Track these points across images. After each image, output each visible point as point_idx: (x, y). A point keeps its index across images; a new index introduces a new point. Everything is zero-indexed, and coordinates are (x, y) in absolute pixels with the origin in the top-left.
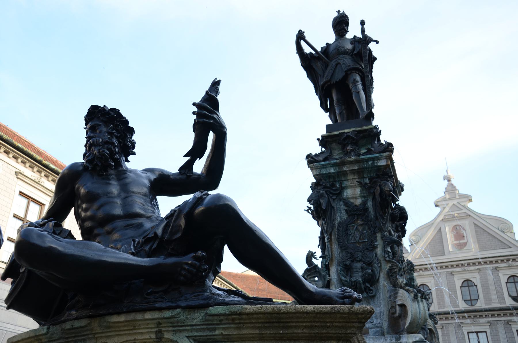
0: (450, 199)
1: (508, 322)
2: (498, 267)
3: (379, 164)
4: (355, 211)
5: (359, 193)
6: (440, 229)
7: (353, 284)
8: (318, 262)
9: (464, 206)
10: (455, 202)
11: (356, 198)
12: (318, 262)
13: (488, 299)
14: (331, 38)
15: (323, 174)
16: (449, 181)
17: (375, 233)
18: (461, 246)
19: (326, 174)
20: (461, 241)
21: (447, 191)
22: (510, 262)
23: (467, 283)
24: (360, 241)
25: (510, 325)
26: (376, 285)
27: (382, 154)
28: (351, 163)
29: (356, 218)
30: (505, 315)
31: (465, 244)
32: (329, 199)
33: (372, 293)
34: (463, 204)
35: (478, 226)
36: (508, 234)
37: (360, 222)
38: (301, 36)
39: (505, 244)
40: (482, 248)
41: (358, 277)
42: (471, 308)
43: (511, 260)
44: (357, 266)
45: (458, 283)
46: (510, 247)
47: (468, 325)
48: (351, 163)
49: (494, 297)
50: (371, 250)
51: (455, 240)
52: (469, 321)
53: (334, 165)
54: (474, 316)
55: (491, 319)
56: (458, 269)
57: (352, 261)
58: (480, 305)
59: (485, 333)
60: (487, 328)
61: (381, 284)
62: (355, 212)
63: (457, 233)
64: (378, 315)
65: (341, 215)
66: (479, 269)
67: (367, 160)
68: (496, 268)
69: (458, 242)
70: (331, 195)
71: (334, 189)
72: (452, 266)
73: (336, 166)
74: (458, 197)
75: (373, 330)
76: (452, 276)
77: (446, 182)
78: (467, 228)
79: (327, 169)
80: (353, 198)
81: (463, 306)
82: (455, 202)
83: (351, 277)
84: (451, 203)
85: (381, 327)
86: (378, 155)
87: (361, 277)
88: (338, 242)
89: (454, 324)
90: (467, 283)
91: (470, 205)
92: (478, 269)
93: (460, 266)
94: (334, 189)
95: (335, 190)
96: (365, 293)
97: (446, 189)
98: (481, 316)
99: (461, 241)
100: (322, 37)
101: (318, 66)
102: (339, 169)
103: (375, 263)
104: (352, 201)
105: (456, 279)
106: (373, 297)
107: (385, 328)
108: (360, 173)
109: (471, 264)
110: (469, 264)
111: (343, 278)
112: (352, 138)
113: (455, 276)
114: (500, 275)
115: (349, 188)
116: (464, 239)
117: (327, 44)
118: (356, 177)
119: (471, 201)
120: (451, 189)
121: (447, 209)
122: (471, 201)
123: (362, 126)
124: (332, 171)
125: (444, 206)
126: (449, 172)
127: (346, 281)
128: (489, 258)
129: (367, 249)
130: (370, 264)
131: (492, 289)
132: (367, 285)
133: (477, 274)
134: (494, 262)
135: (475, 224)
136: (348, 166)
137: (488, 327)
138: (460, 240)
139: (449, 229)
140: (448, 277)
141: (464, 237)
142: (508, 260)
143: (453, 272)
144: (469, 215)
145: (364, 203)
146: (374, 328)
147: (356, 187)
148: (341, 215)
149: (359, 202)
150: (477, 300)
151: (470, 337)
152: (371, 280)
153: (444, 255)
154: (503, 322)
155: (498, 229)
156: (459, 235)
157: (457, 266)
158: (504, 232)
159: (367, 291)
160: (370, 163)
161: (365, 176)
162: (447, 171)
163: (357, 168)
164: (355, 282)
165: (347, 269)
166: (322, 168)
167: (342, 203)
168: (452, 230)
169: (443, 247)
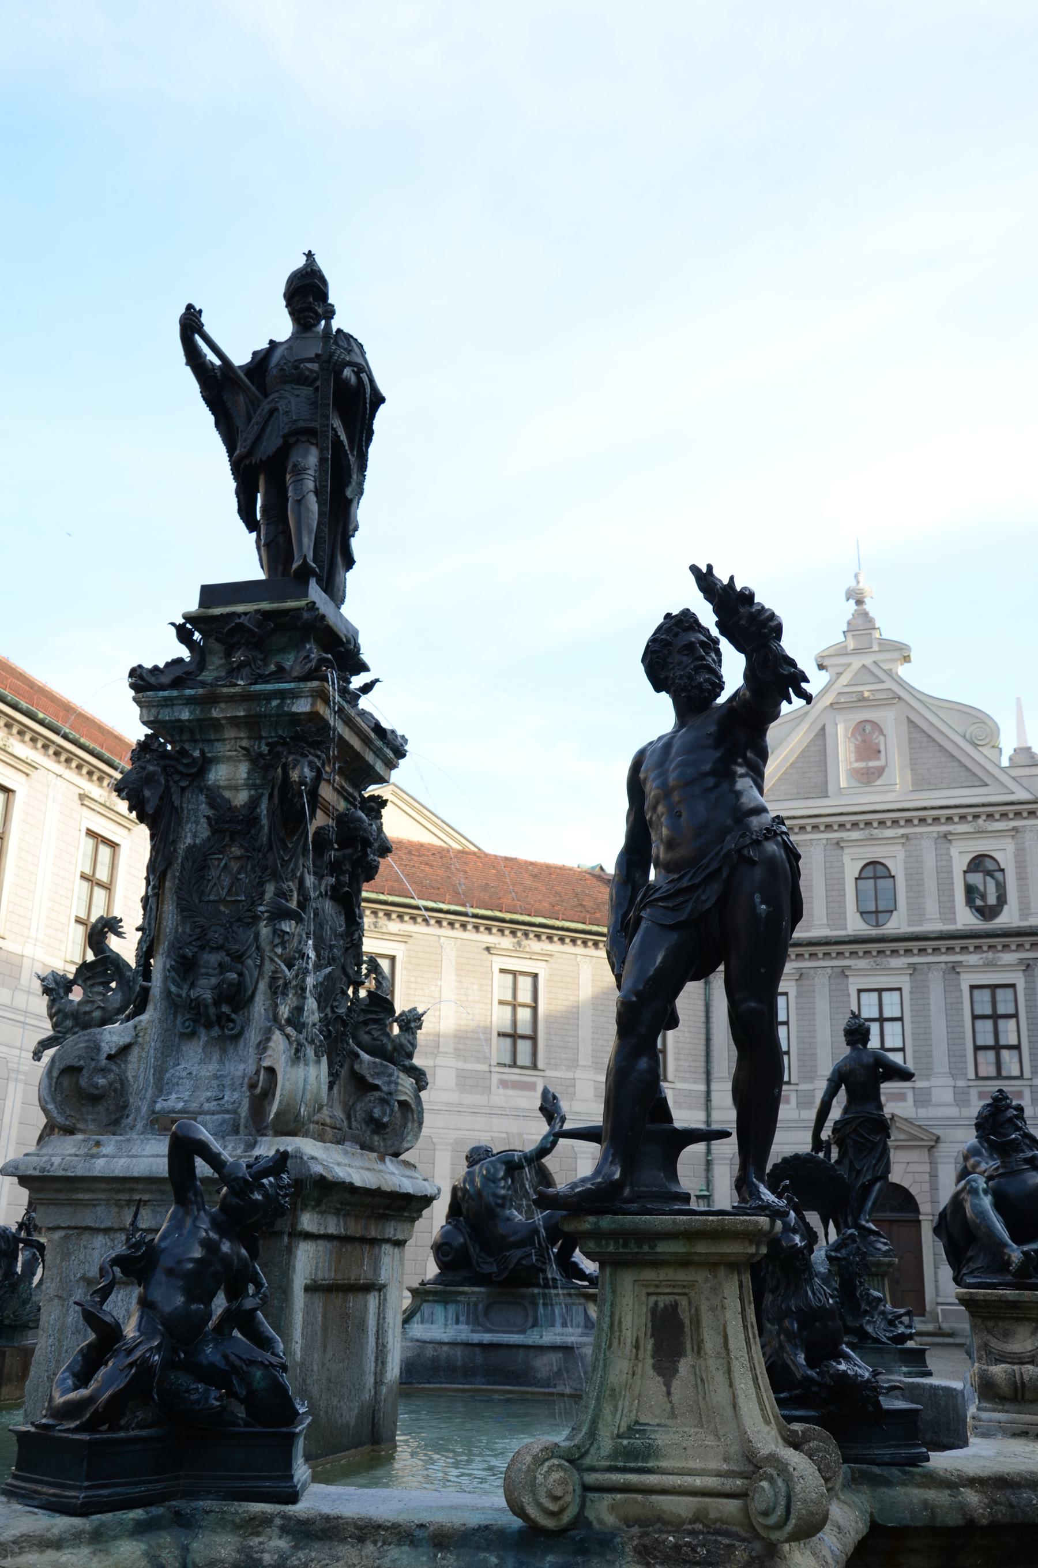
0: (857, 651)
1: (953, 968)
2: (951, 833)
3: (295, 709)
4: (228, 822)
5: (245, 776)
6: (823, 729)
7: (193, 1005)
8: (125, 947)
9: (889, 673)
10: (868, 660)
11: (235, 788)
12: (125, 947)
13: (917, 912)
14: (281, 327)
15: (165, 722)
16: (859, 602)
17: (262, 884)
18: (868, 776)
19: (170, 721)
20: (873, 764)
21: (851, 629)
22: (980, 821)
23: (875, 871)
24: (228, 898)
25: (958, 973)
26: (246, 1010)
27: (302, 685)
28: (231, 699)
29: (227, 839)
30: (950, 950)
31: (880, 771)
32: (167, 787)
33: (232, 1029)
34: (886, 667)
35: (916, 726)
36: (986, 751)
37: (236, 851)
38: (191, 324)
39: (974, 774)
40: (920, 784)
41: (204, 990)
42: (874, 932)
43: (984, 817)
44: (208, 962)
45: (852, 869)
46: (987, 785)
47: (861, 972)
48: (231, 699)
49: (932, 907)
50: (249, 924)
51: (857, 760)
52: (862, 963)
53: (190, 701)
54: (879, 952)
55: (916, 960)
56: (855, 835)
57: (202, 948)
58: (897, 924)
59: (897, 993)
60: (904, 982)
61: (257, 1009)
62: (227, 826)
63: (864, 741)
64: (238, 1083)
65: (195, 832)
66: (906, 837)
67: (269, 696)
68: (945, 836)
69: (863, 765)
70: (177, 777)
71: (185, 761)
72: (842, 826)
73: (196, 704)
74: (876, 648)
75: (216, 1117)
76: (839, 852)
77: (852, 605)
79: (176, 708)
80: (229, 787)
81: (855, 925)
82: (868, 660)
83: (192, 986)
84: (857, 662)
85: (235, 1112)
86: (292, 685)
87: (213, 989)
88: (178, 898)
89: (829, 970)
90: (875, 871)
91: (904, 671)
92: (903, 836)
93: (862, 826)
94: (185, 761)
95: (187, 766)
96: (216, 1028)
97: (849, 623)
98: (894, 952)
99: (873, 764)
100: (251, 326)
101: (239, 404)
102: (202, 711)
103: (249, 957)
104: (227, 794)
105: (846, 859)
106: (237, 1037)
107: (243, 1115)
108: (251, 724)
109: (889, 823)
110: (882, 823)
111: (173, 989)
112: (250, 631)
113: (846, 851)
114: (954, 852)
115: (223, 762)
116: (879, 759)
117: (271, 342)
118: (242, 735)
119: (907, 659)
120: (862, 625)
121: (845, 679)
122: (907, 659)
123: (283, 599)
124: (185, 715)
125: (840, 669)
126: (861, 579)
127: (180, 996)
128: (933, 808)
129: (239, 920)
130: (239, 958)
131: (931, 886)
132: (226, 1009)
133: (900, 847)
134: (943, 820)
135: (910, 721)
136: (223, 705)
137: (907, 978)
138: (870, 759)
139: (846, 730)
140: (828, 853)
141: (879, 752)
142: (976, 817)
143: (842, 840)
144: (899, 698)
145: (253, 803)
146: (218, 1113)
147: (240, 761)
148: (195, 832)
149: (241, 798)
150: (891, 912)
151: (862, 1002)
152: (236, 998)
153: (827, 797)
154: (943, 966)
155: (964, 737)
156: (868, 747)
157: (855, 825)
158: (976, 745)
159: (223, 1022)
160: (275, 703)
161: (264, 734)
162: (856, 576)
163: (242, 714)
164: (197, 998)
165: (185, 968)
166: (163, 706)
167: (202, 798)
168: (853, 734)
169: (826, 776)
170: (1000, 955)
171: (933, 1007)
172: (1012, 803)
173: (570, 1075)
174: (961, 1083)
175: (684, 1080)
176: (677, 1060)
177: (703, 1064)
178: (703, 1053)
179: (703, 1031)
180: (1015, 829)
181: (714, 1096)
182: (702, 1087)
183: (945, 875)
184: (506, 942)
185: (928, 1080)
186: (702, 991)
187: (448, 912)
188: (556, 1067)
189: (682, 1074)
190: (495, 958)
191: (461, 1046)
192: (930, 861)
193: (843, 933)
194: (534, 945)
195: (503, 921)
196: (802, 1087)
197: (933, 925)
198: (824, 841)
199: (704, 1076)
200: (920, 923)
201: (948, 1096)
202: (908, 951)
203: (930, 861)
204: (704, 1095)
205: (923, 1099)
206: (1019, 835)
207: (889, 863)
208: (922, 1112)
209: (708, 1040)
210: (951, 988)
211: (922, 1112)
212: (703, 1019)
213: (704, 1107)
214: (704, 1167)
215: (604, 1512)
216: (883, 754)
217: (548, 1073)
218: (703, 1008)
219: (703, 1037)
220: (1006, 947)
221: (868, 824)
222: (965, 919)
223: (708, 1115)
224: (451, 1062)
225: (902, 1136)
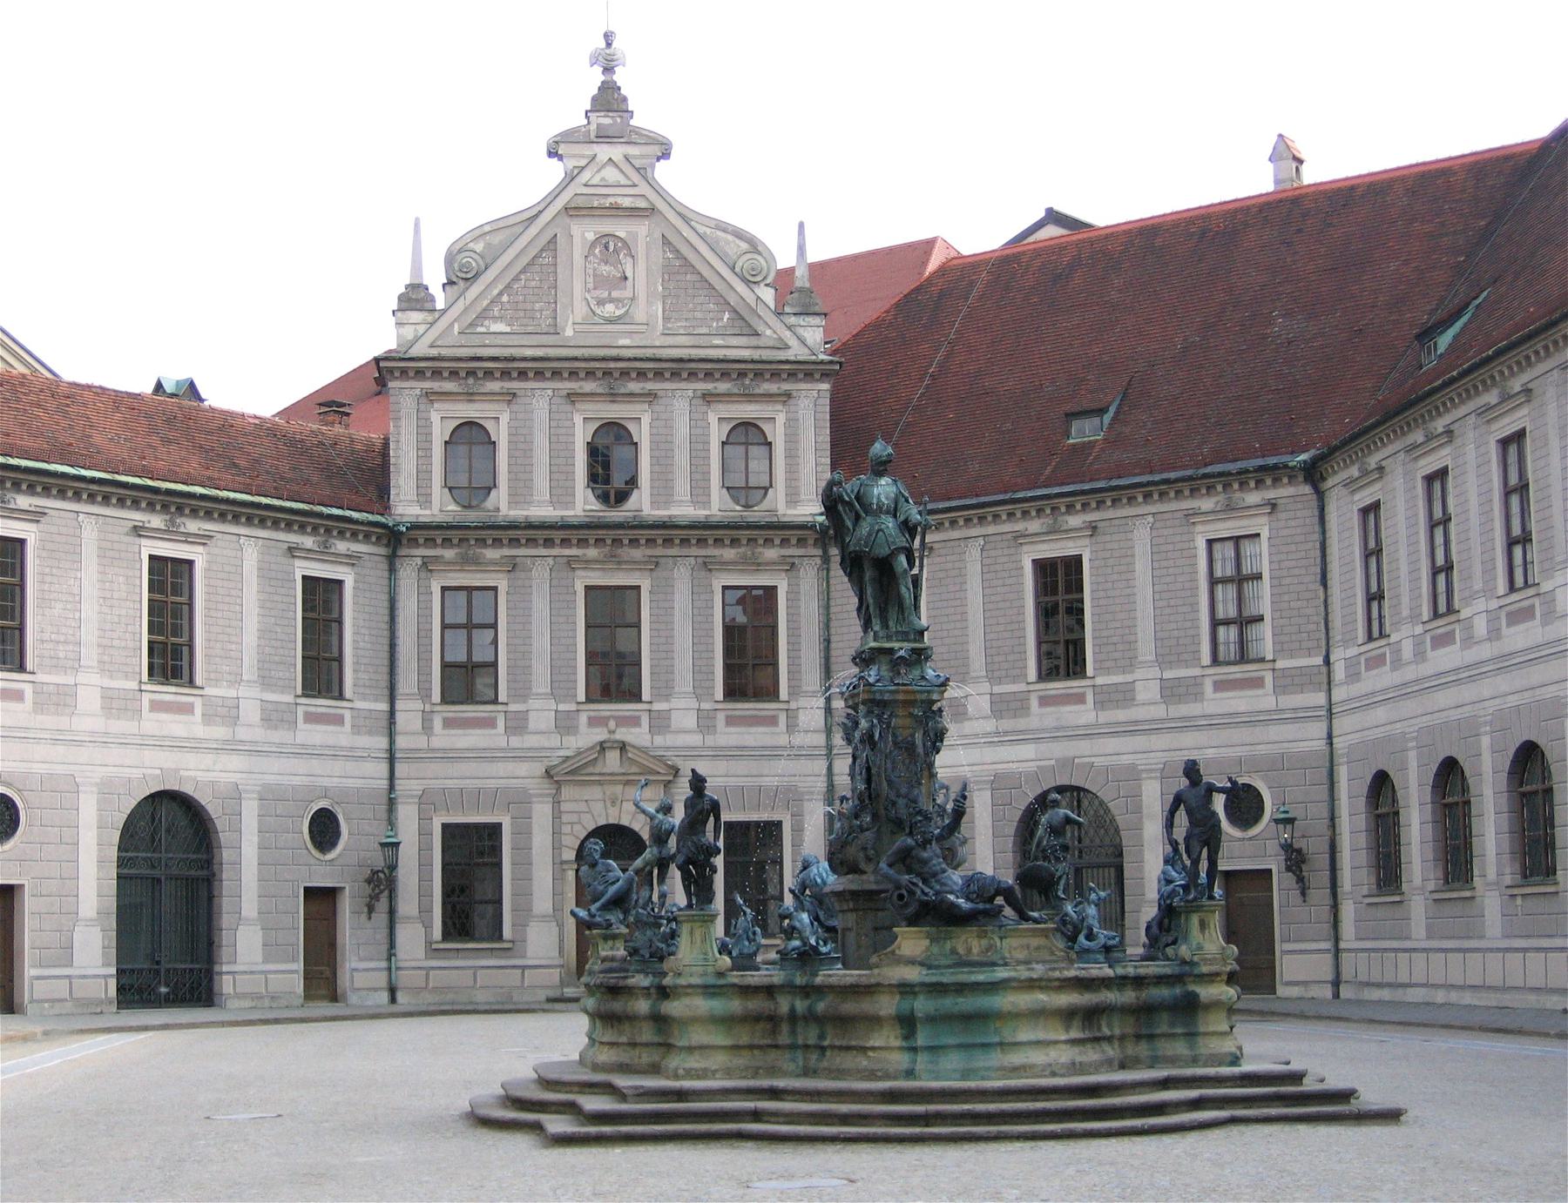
0: (604, 137)
16: (608, 70)
22: (747, 382)
34: (637, 163)
43: (751, 376)
49: (682, 487)
68: (704, 396)
76: (569, 408)
77: (596, 77)
78: (641, 251)
91: (663, 172)
98: (634, 542)
110: (625, 373)
114: (713, 418)
120: (609, 99)
122: (666, 155)
125: (583, 163)
131: (682, 460)
142: (742, 374)
144: (652, 211)
170: (760, 549)
171: (676, 612)
172: (787, 362)
173: (232, 693)
174: (706, 706)
175: (364, 697)
176: (355, 671)
177: (386, 677)
178: (386, 662)
179: (386, 633)
180: (788, 395)
181: (399, 717)
182: (384, 706)
183: (700, 446)
184: (156, 521)
185: (667, 701)
186: (386, 582)
187: (93, 481)
188: (216, 682)
189: (361, 690)
190: (144, 542)
191: (106, 658)
192: (682, 429)
193: (571, 513)
194: (193, 526)
195: (156, 491)
196: (513, 707)
197: (683, 510)
198: (550, 392)
199: (386, 692)
200: (667, 504)
201: (690, 721)
202: (651, 542)
203: (682, 429)
204: (386, 716)
205: (660, 723)
206: (792, 402)
207: (631, 427)
208: (659, 740)
209: (393, 646)
210: (700, 591)
211: (659, 740)
212: (387, 618)
213: (386, 731)
214: (385, 807)
215: (1196, 959)
216: (629, 283)
217: (208, 691)
218: (386, 604)
219: (386, 641)
220: (768, 542)
221: (607, 373)
222: (718, 505)
223: (392, 742)
224: (95, 679)
225: (634, 769)
